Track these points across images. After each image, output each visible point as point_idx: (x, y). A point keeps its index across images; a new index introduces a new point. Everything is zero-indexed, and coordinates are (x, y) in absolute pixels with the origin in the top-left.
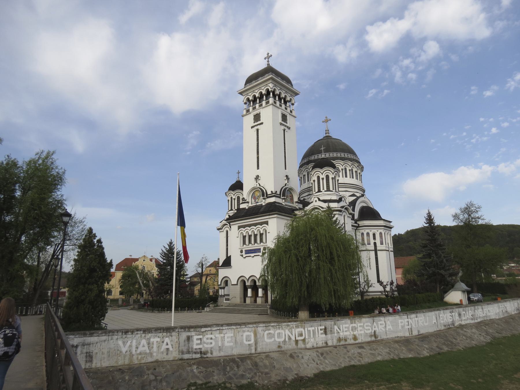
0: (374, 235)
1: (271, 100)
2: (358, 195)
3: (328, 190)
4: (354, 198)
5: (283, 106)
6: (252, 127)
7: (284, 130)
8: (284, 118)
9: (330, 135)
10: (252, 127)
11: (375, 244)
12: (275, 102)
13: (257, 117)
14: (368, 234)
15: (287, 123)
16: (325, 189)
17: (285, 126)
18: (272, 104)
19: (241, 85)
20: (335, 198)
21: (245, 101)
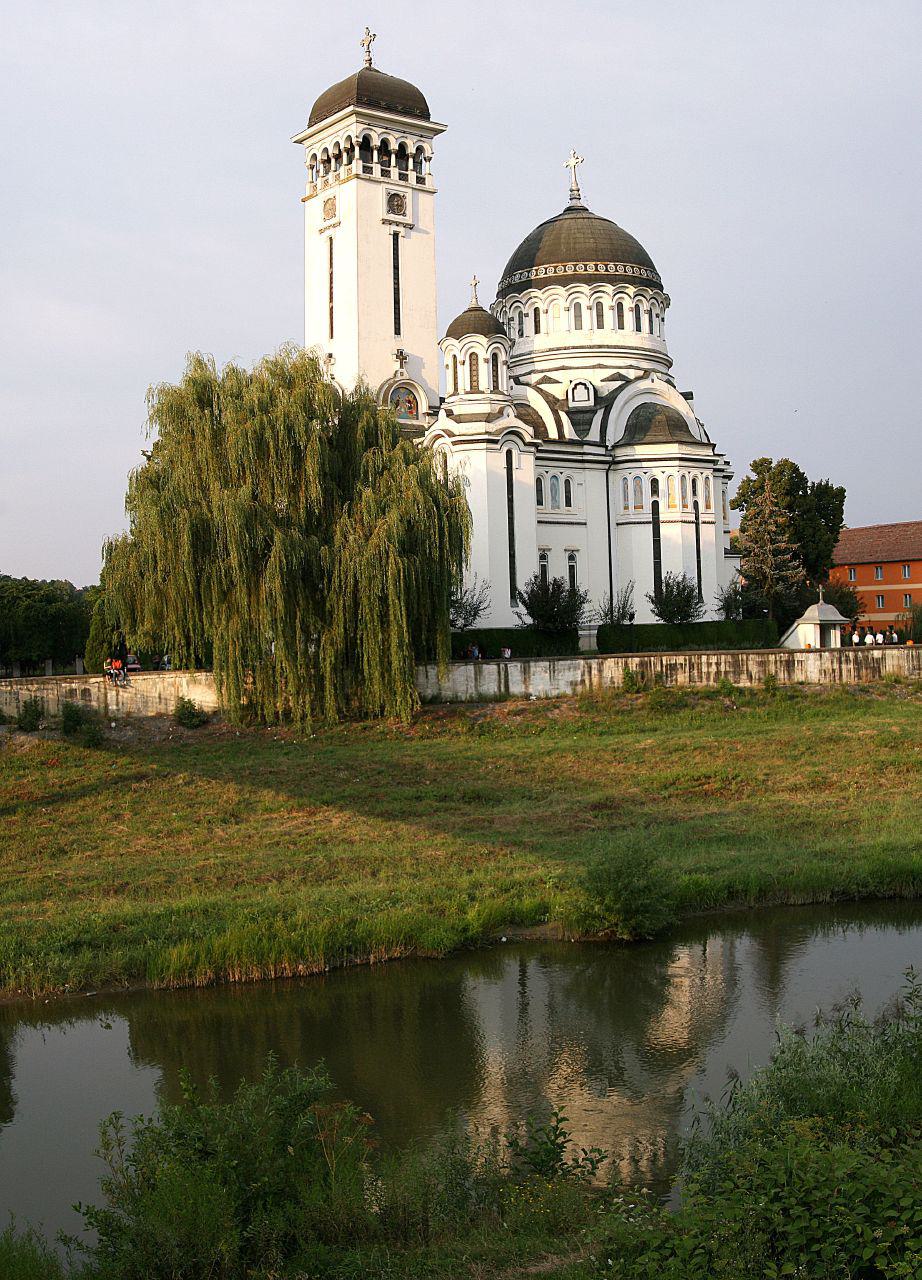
0: (655, 482)
1: (357, 166)
2: (632, 374)
3: (474, 389)
4: (619, 383)
5: (395, 172)
6: (321, 231)
7: (396, 236)
8: (395, 203)
9: (583, 203)
10: (321, 231)
11: (655, 505)
12: (367, 170)
13: (330, 207)
15: (404, 214)
16: (468, 389)
18: (357, 176)
19: (301, 125)
20: (486, 409)
21: (308, 163)
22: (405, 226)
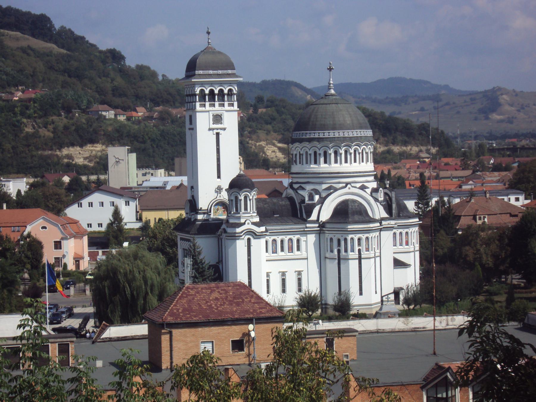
0: (339, 241)
7: (218, 134)
11: (339, 251)
14: (331, 239)
17: (217, 129)
22: (221, 129)
